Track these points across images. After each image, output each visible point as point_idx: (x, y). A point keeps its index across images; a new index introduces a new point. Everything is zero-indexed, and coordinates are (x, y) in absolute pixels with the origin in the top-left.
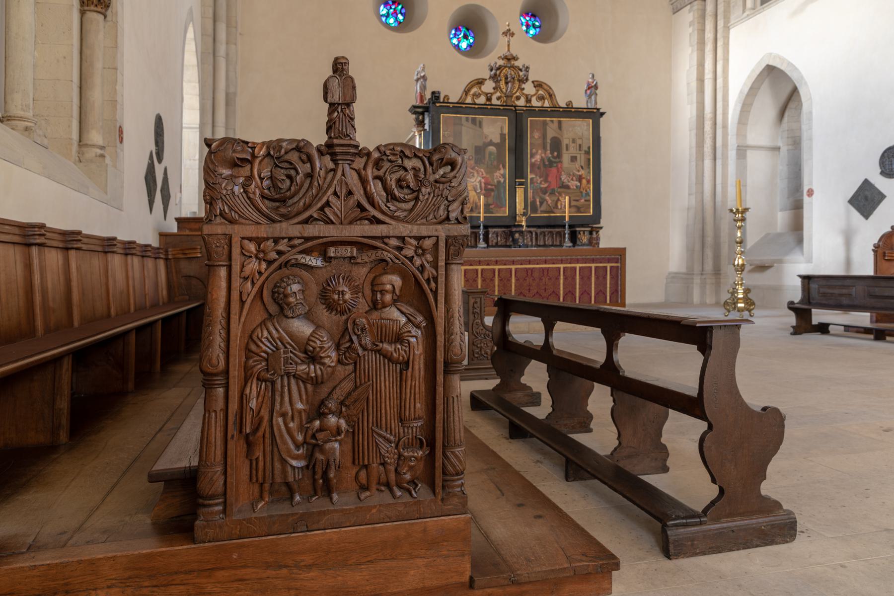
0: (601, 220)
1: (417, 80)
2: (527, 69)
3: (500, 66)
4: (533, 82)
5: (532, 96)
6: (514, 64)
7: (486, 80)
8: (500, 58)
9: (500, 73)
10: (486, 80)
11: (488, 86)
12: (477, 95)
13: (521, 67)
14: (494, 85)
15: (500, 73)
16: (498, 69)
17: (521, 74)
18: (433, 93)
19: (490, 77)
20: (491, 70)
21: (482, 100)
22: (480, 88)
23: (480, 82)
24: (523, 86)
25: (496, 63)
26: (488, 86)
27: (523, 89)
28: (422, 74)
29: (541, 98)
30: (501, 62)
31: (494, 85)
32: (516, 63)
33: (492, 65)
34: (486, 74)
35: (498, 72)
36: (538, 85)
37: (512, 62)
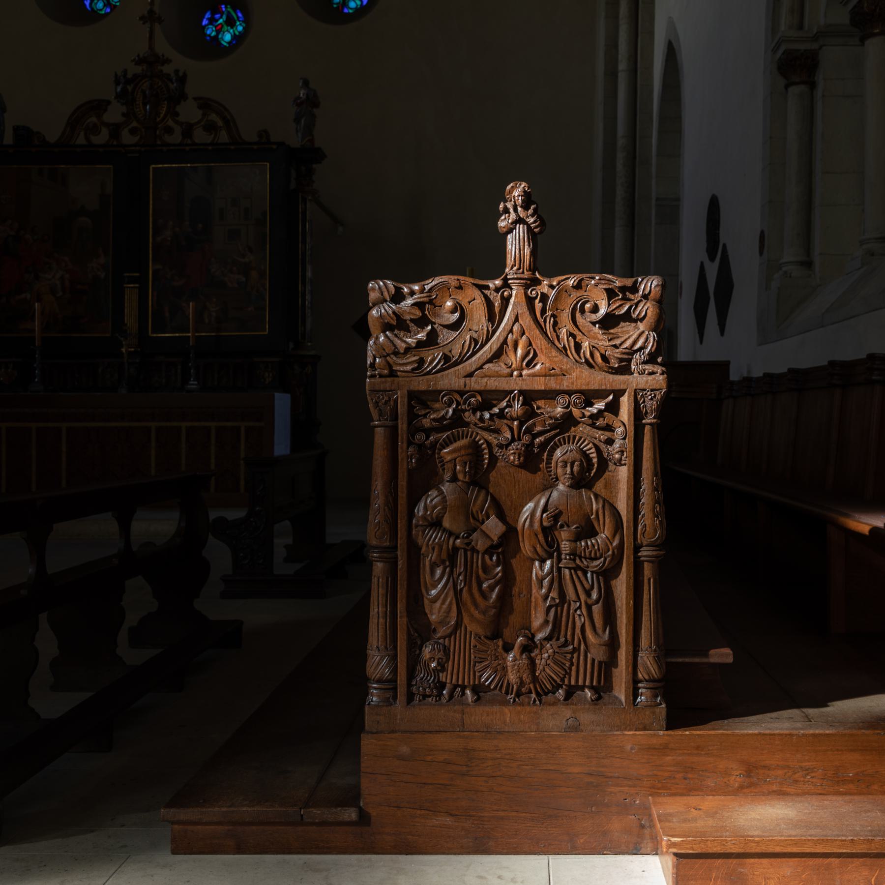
7: (109, 103)
10: (109, 103)
11: (115, 114)
14: (124, 109)
18: (16, 129)
20: (117, 83)
21: (102, 137)
23: (99, 106)
25: (125, 71)
26: (115, 114)
27: (177, 114)
29: (210, 128)
30: (138, 70)
31: (124, 109)
32: (167, 69)
35: (130, 88)
36: (205, 104)
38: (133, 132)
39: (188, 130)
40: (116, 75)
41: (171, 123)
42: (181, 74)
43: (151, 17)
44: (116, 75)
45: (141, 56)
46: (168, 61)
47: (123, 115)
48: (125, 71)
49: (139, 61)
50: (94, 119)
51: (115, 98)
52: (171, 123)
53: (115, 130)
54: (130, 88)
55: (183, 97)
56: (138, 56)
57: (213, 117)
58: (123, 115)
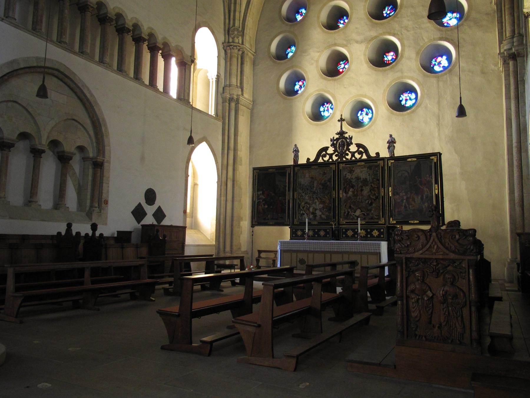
0: (90, 227)
1: (293, 152)
2: (351, 138)
3: (336, 138)
4: (355, 144)
5: (355, 152)
6: (344, 136)
7: (329, 147)
8: (336, 134)
9: (337, 143)
10: (329, 147)
11: (331, 150)
12: (325, 156)
13: (348, 137)
14: (333, 149)
15: (337, 143)
16: (335, 140)
17: (348, 141)
19: (331, 145)
20: (331, 140)
21: (326, 159)
22: (326, 152)
23: (326, 149)
24: (350, 147)
25: (334, 137)
26: (331, 150)
27: (350, 149)
28: (295, 149)
29: (360, 153)
30: (337, 136)
31: (333, 149)
32: (346, 135)
33: (332, 138)
34: (328, 144)
35: (335, 142)
36: (359, 146)
37: (344, 135)
38: (336, 156)
39: (353, 154)
40: (331, 139)
41: (347, 152)
42: (351, 137)
43: (341, 120)
44: (331, 139)
45: (338, 132)
46: (347, 133)
47: (333, 151)
48: (334, 137)
49: (337, 134)
50: (324, 153)
51: (331, 146)
52: (347, 152)
53: (331, 156)
54: (335, 142)
55: (352, 144)
56: (337, 132)
57: (361, 149)
58: (333, 151)
